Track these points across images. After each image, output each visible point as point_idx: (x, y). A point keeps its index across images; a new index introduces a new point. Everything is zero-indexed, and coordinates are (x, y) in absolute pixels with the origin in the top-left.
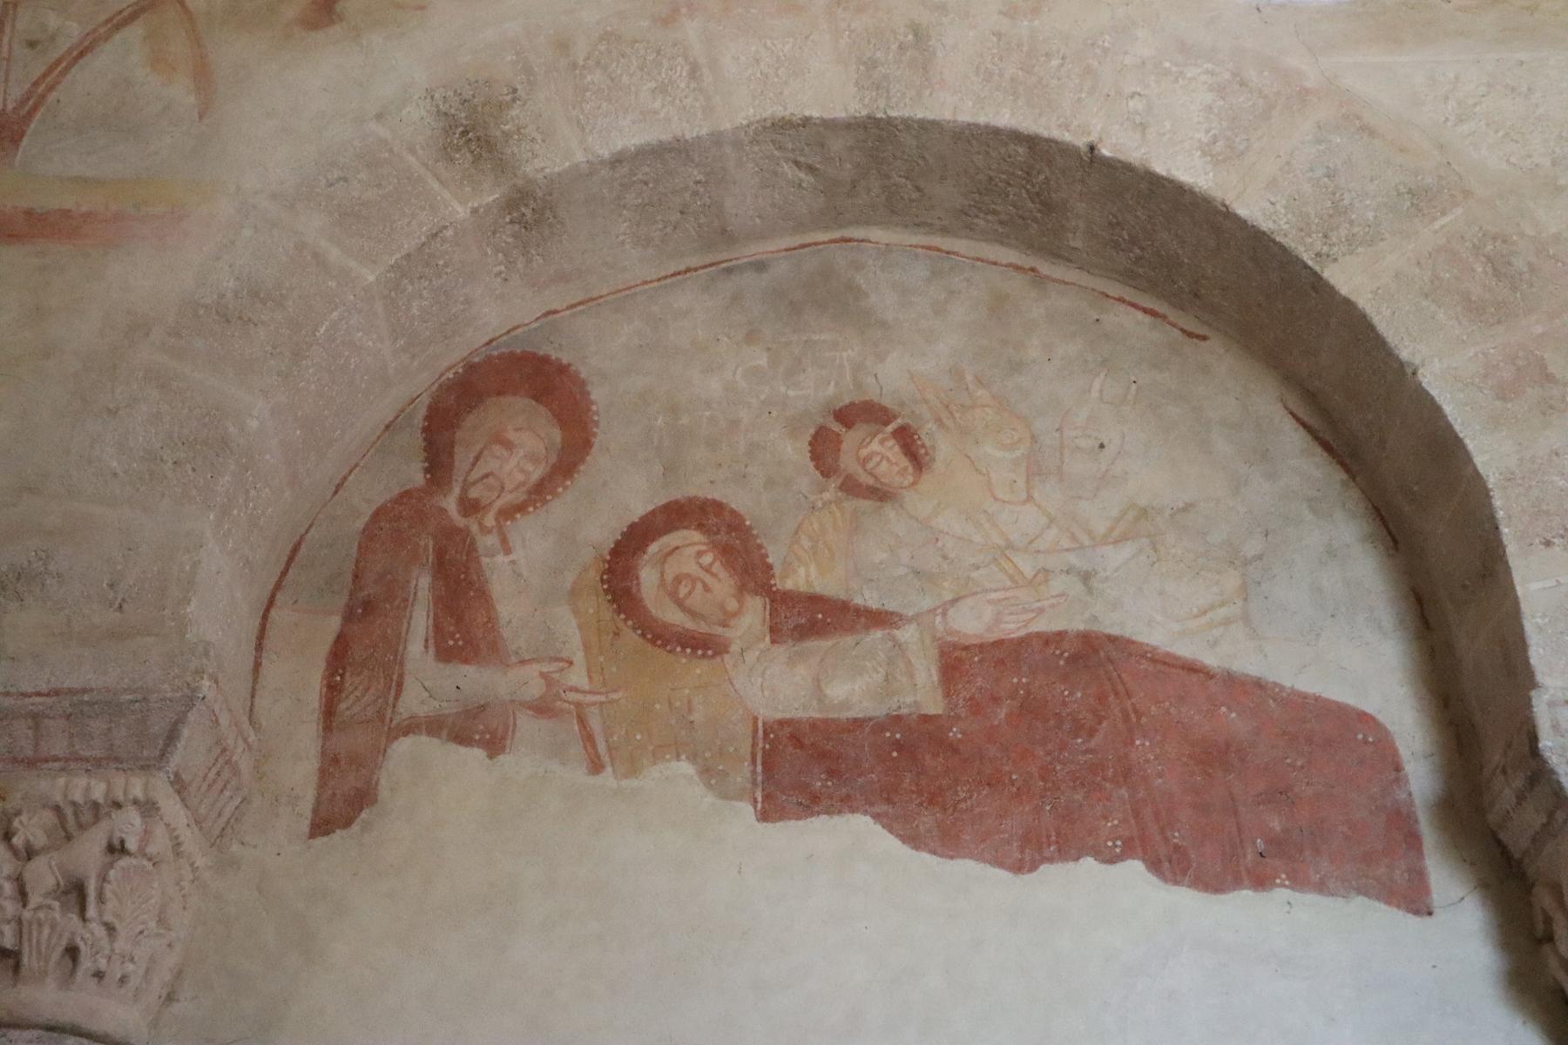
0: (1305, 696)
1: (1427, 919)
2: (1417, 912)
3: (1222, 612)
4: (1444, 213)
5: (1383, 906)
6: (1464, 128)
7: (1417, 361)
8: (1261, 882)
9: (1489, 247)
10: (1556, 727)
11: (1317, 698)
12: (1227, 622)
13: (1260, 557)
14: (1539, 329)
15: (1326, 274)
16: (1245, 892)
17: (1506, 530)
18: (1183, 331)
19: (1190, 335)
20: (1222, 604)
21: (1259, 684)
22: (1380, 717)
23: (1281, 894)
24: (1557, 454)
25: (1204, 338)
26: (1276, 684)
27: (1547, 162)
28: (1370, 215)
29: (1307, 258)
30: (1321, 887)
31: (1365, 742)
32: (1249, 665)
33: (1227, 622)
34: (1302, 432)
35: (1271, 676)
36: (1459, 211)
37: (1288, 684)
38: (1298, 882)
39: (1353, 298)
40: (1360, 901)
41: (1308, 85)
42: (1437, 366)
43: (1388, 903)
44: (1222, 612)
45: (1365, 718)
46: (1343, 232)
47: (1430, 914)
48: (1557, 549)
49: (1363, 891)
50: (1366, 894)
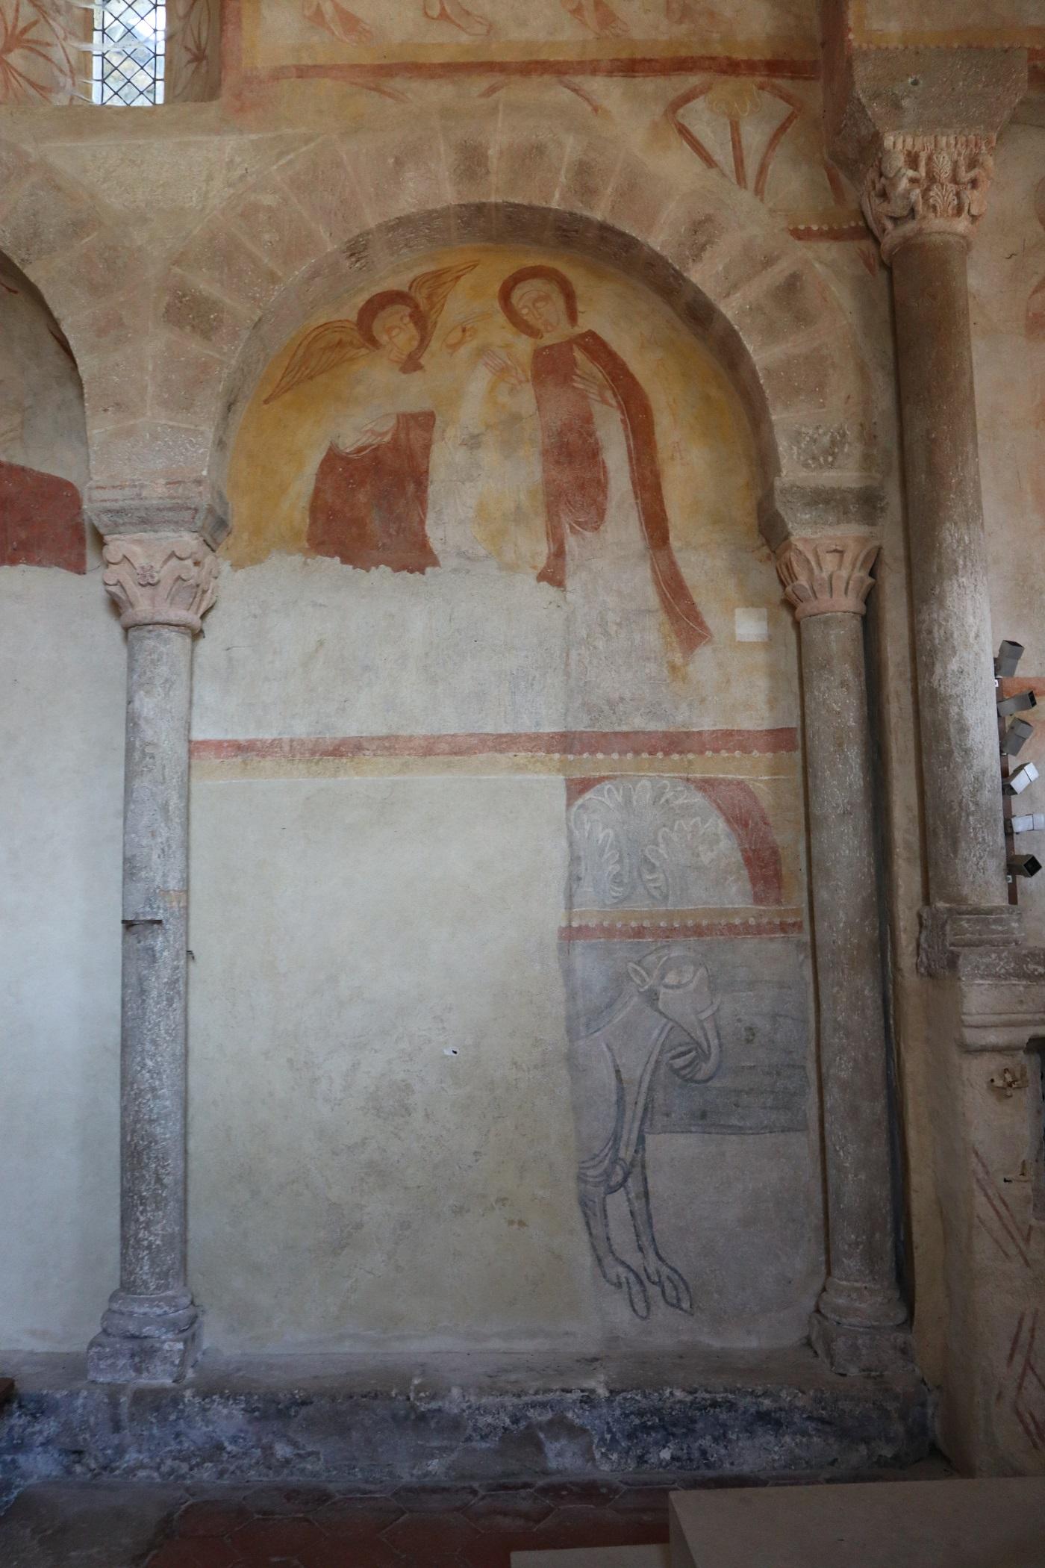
0: (43, 474)
1: (77, 577)
2: (79, 573)
3: (11, 434)
4: (88, 236)
5: (65, 571)
6: (105, 186)
7: (61, 317)
8: (13, 562)
9: (107, 254)
10: (90, 500)
11: (49, 476)
12: (13, 439)
13: (30, 407)
14: (122, 299)
15: (25, 271)
16: (5, 567)
17: (87, 404)
18: (7, 288)
19: (10, 290)
20: (11, 431)
21: (23, 469)
22: (75, 484)
23: (22, 567)
24: (117, 365)
25: (16, 292)
26: (31, 469)
27: (143, 205)
28: (51, 236)
29: (16, 262)
30: (39, 563)
31: (67, 496)
32: (19, 460)
33: (13, 439)
34: (55, 342)
35: (29, 466)
36: (95, 234)
37: (36, 468)
38: (30, 561)
39: (36, 284)
40: (56, 569)
41: (31, 161)
42: (70, 320)
43: (68, 569)
44: (11, 434)
45: (69, 485)
46: (36, 247)
47: (84, 574)
48: (109, 413)
49: (58, 565)
50: (59, 566)
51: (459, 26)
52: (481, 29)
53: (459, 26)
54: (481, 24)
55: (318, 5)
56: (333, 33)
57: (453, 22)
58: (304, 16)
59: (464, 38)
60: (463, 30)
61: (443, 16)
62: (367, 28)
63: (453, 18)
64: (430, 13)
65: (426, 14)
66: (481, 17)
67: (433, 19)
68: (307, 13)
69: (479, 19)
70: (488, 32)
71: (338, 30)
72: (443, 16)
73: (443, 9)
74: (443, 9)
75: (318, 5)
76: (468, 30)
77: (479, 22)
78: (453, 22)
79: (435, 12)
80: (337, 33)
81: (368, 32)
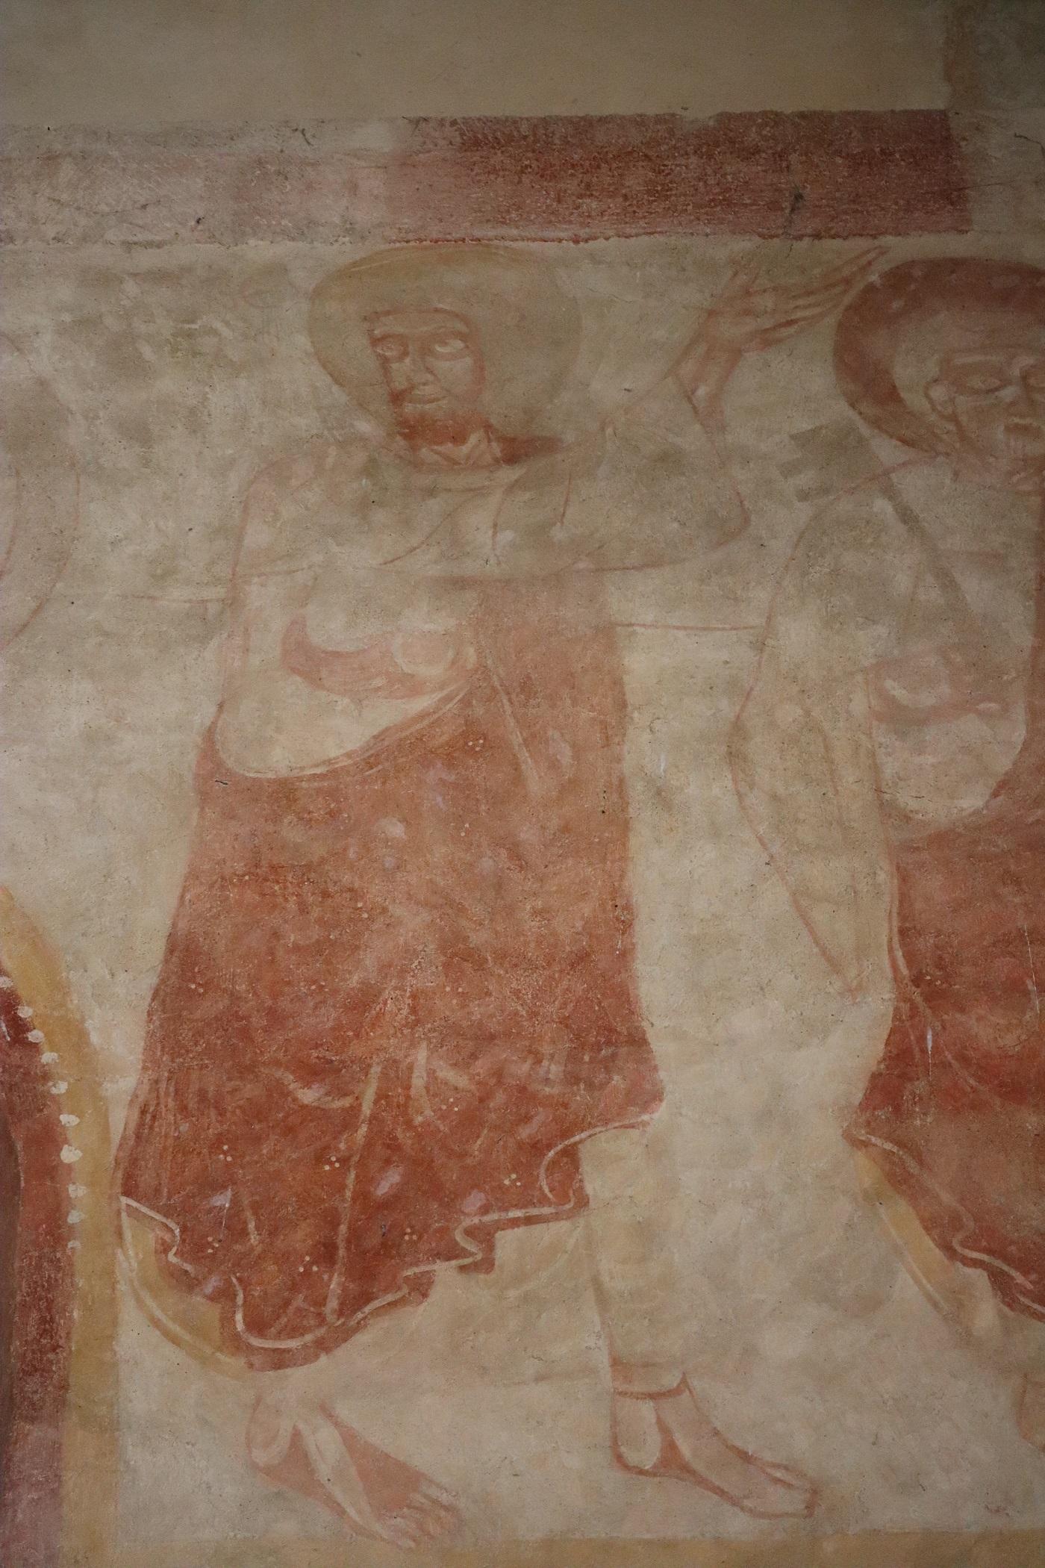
51: (721, 1492)
52: (789, 1502)
53: (721, 1492)
54: (789, 1486)
55: (296, 1435)
56: (342, 1512)
57: (702, 1482)
58: (254, 1467)
59: (738, 1526)
60: (735, 1502)
61: (671, 1463)
62: (444, 1498)
63: (699, 1466)
64: (632, 1457)
65: (619, 1458)
66: (786, 1468)
67: (642, 1472)
68: (261, 1457)
69: (778, 1474)
70: (810, 1507)
71: (356, 1507)
72: (671, 1463)
73: (670, 1446)
74: (670, 1446)
75: (296, 1435)
76: (747, 1503)
77: (777, 1481)
78: (702, 1482)
79: (648, 1455)
80: (351, 1511)
81: (447, 1508)
